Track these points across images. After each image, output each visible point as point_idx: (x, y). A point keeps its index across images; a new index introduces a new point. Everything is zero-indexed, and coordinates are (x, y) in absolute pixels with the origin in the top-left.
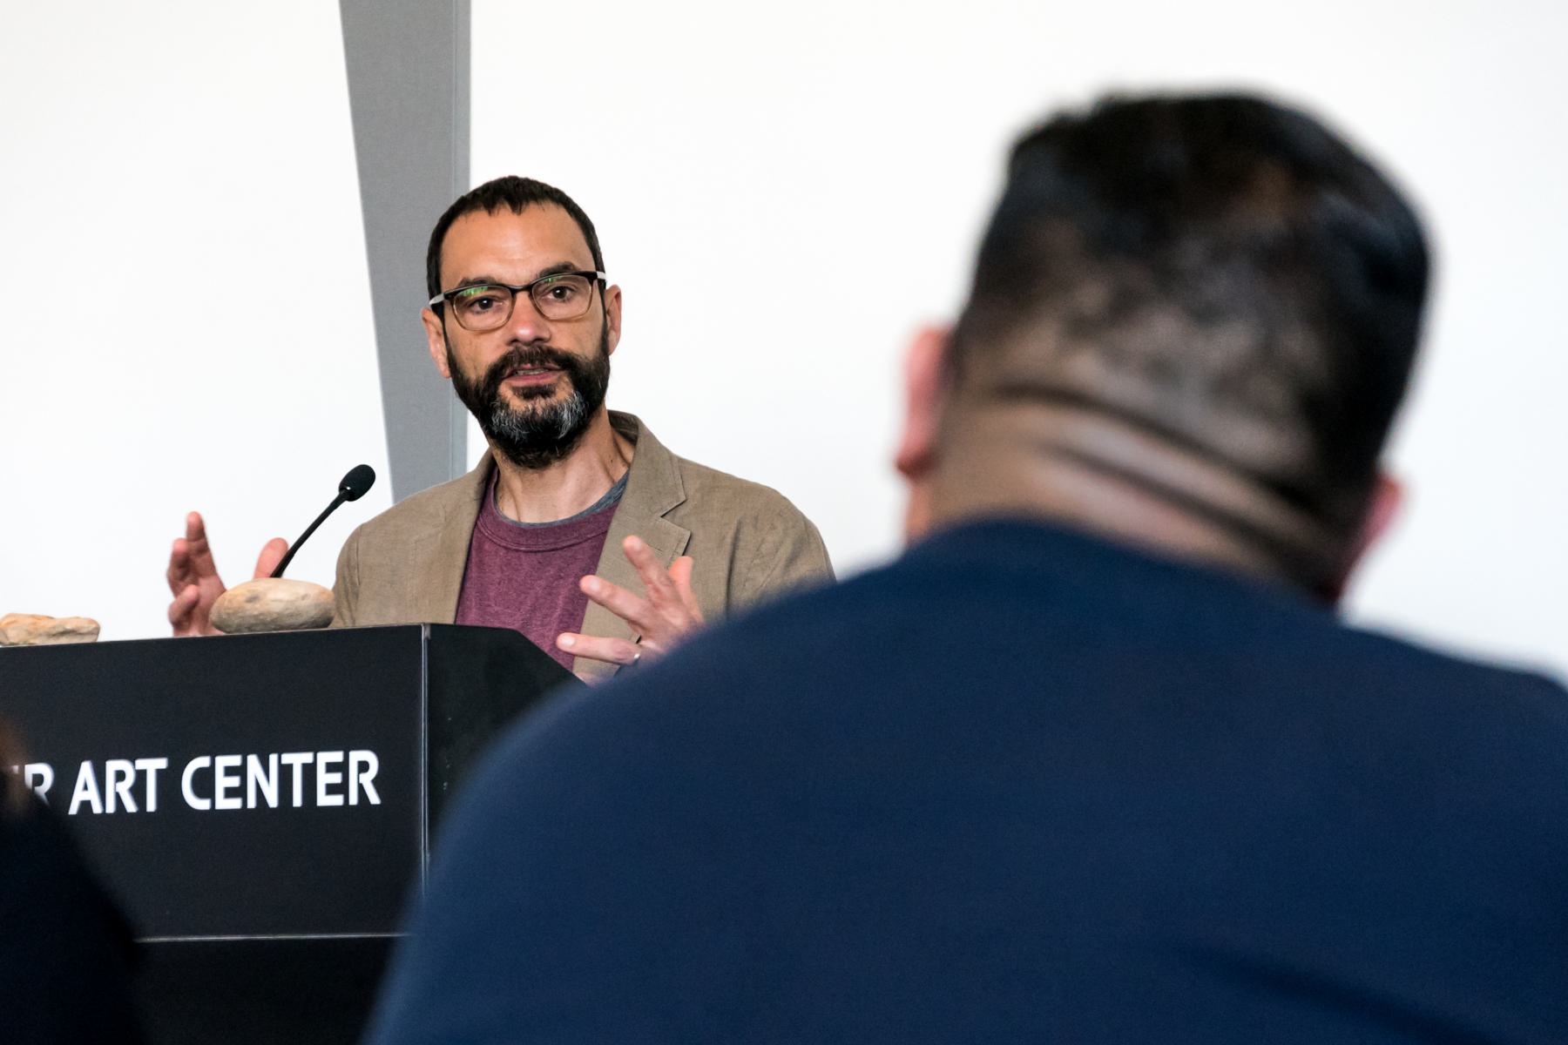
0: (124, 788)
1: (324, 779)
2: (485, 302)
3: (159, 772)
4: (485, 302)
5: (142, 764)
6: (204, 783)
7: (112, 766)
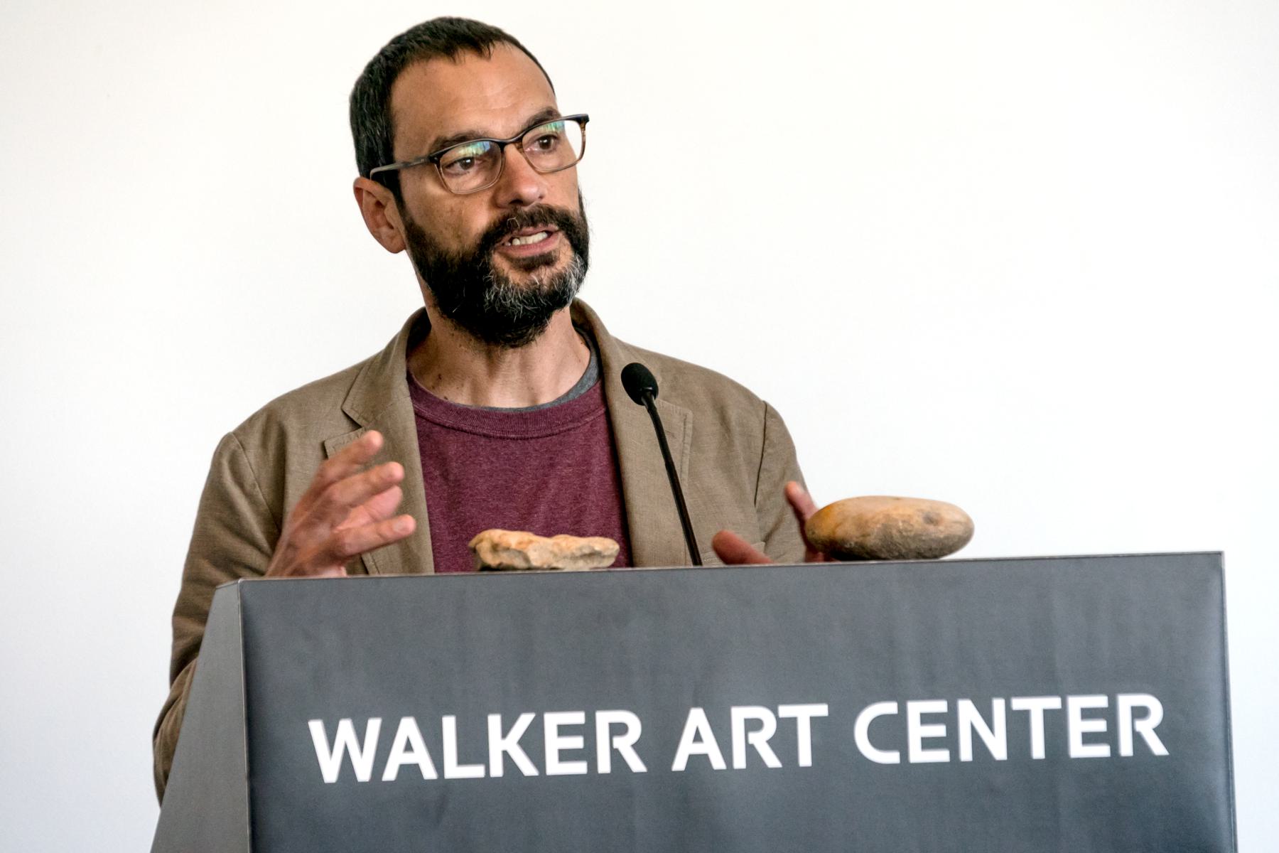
0: (760, 740)
1: (1077, 727)
2: (469, 161)
3: (814, 720)
4: (469, 161)
5: (786, 711)
7: (739, 715)
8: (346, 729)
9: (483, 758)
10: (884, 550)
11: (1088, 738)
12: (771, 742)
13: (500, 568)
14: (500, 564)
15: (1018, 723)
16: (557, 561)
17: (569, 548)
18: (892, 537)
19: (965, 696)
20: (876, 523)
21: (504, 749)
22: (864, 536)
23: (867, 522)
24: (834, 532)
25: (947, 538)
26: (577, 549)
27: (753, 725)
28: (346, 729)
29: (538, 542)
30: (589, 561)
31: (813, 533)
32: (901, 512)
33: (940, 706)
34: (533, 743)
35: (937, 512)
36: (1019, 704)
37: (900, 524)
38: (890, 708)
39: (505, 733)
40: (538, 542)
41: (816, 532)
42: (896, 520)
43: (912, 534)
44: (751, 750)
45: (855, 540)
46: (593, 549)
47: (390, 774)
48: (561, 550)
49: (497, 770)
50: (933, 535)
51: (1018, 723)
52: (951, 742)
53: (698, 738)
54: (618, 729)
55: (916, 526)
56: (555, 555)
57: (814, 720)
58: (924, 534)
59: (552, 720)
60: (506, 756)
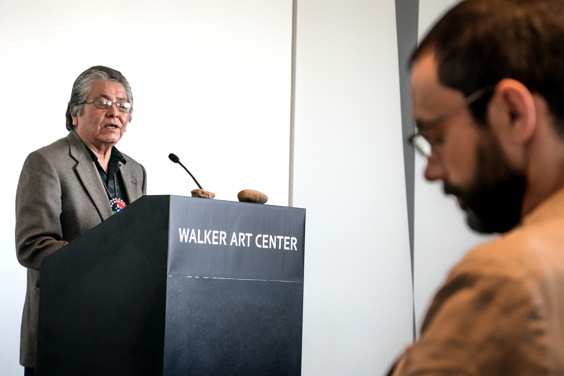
1: (286, 243)
5: (247, 234)
6: (260, 241)
7: (241, 234)
13: (204, 197)
27: (242, 237)
45: (254, 199)
47: (190, 242)
59: (214, 232)
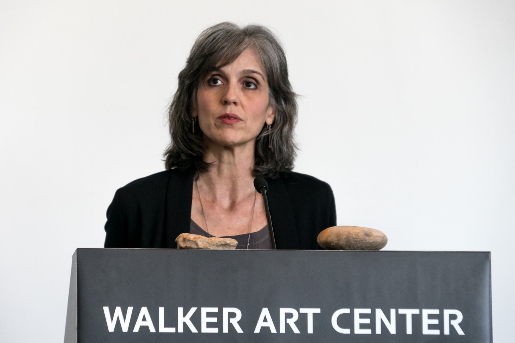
0: (291, 322)
1: (426, 322)
3: (314, 315)
5: (302, 310)
7: (283, 311)
8: (118, 310)
9: (176, 326)
10: (347, 246)
11: (431, 327)
12: (296, 323)
13: (186, 247)
14: (186, 246)
15: (401, 320)
16: (210, 246)
17: (215, 241)
18: (350, 241)
19: (378, 308)
20: (344, 235)
21: (184, 321)
22: (338, 240)
23: (340, 235)
24: (327, 239)
25: (373, 242)
26: (219, 242)
27: (289, 316)
28: (118, 310)
29: (202, 238)
30: (224, 247)
31: (319, 240)
32: (354, 231)
33: (368, 311)
34: (196, 319)
35: (370, 232)
36: (401, 311)
37: (354, 236)
38: (347, 311)
39: (184, 315)
40: (201, 238)
41: (320, 239)
42: (352, 234)
43: (359, 240)
44: (287, 326)
45: (335, 242)
46: (226, 242)
47: (136, 329)
48: (212, 242)
49: (181, 330)
50: (368, 241)
51: (401, 320)
52: (372, 326)
53: (144, 319)
54: (232, 315)
55: (361, 237)
56: (209, 244)
57: (314, 315)
58: (364, 240)
59: (204, 310)
60: (184, 323)
